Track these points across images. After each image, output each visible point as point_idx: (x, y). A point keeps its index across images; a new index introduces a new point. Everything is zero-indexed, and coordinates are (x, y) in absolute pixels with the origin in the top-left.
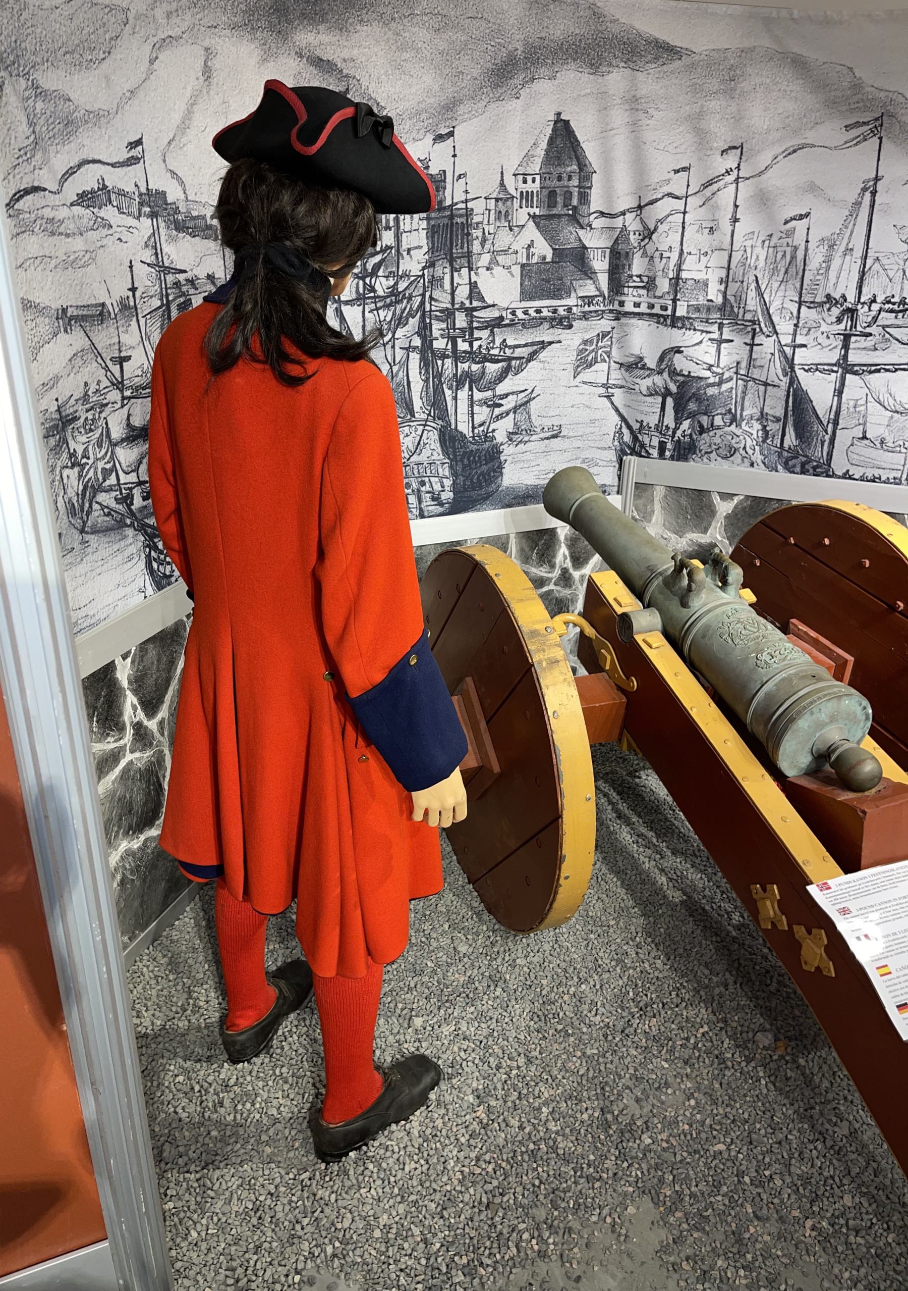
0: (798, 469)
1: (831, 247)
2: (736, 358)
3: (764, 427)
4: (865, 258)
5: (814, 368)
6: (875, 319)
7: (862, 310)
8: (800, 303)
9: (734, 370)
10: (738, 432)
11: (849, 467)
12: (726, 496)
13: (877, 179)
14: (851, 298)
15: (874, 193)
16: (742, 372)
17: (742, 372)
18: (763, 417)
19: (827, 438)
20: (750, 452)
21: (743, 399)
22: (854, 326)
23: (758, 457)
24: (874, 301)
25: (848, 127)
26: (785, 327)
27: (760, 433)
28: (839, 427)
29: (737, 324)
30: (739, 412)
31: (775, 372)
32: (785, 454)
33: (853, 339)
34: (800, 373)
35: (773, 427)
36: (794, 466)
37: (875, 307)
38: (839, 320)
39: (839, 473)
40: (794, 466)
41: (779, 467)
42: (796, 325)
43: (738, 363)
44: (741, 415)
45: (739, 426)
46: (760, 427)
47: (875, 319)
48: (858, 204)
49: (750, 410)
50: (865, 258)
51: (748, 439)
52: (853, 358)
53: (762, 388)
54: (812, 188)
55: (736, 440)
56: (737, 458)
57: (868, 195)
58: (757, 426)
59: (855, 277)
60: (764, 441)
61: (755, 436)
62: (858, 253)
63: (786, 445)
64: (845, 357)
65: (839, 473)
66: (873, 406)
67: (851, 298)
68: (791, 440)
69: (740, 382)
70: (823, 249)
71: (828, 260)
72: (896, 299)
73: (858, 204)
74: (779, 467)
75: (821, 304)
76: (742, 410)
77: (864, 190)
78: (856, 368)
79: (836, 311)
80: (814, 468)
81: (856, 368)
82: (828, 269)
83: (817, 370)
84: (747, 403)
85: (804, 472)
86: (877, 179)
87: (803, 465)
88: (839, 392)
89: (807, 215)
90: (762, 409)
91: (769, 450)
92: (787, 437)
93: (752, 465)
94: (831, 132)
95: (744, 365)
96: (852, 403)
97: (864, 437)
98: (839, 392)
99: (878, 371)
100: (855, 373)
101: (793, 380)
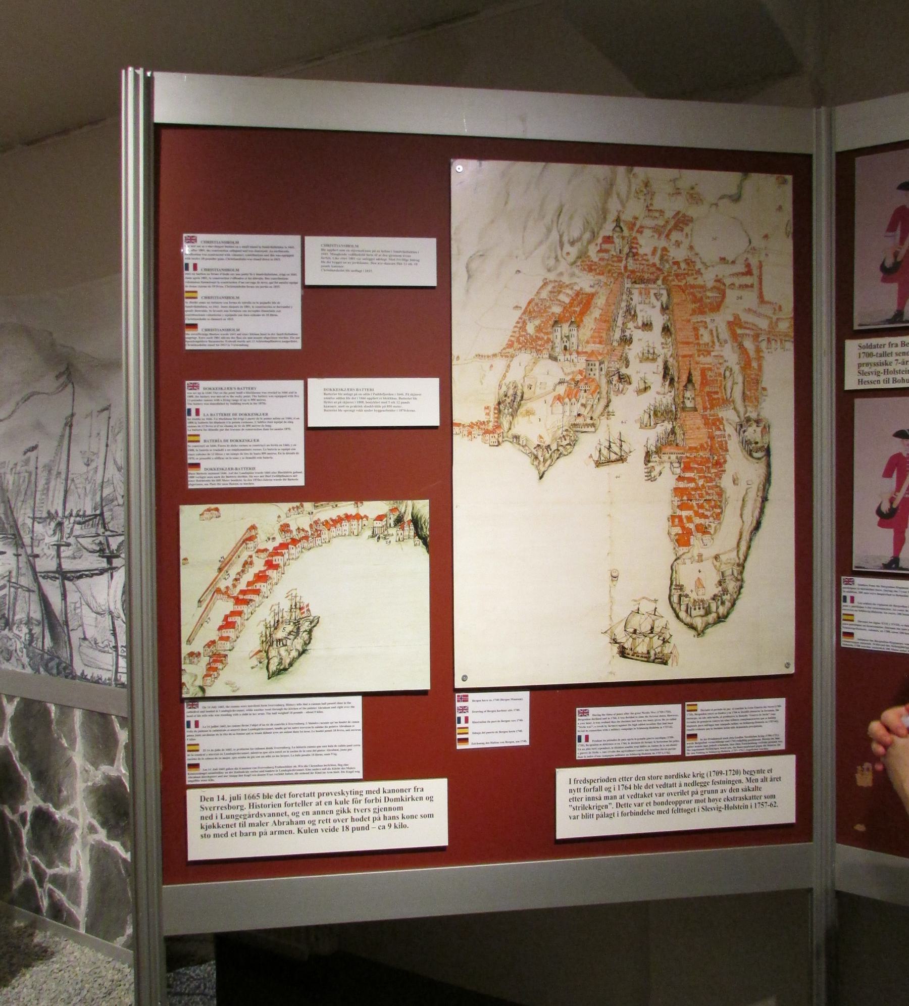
0: (55, 671)
1: (50, 471)
2: (8, 567)
3: (31, 630)
4: (67, 479)
5: (47, 575)
6: (72, 529)
7: (66, 523)
8: (34, 519)
9: (7, 579)
10: (10, 635)
11: (83, 667)
12: (10, 698)
13: (73, 415)
14: (60, 514)
15: (71, 426)
16: (13, 580)
17: (13, 580)
18: (29, 622)
19: (66, 638)
20: (20, 654)
21: (14, 604)
22: (62, 538)
23: (26, 660)
24: (71, 515)
25: (57, 377)
26: (27, 540)
27: (28, 636)
28: (71, 628)
29: (8, 538)
30: (11, 617)
31: (26, 581)
32: (46, 656)
33: (62, 548)
34: (41, 579)
35: (37, 630)
36: (52, 668)
37: (72, 519)
38: (54, 534)
39: (79, 674)
40: (52, 668)
41: (41, 669)
42: (32, 538)
43: (10, 572)
44: (13, 620)
45: (11, 629)
46: (27, 631)
47: (72, 529)
48: (62, 436)
49: (20, 616)
50: (67, 479)
51: (18, 643)
52: (67, 565)
53: (27, 593)
54: (39, 426)
55: (9, 643)
56: (13, 660)
57: (68, 428)
58: (25, 630)
59: (62, 494)
60: (30, 644)
61: (23, 639)
62: (63, 476)
63: (46, 648)
64: (60, 565)
65: (79, 674)
66: (85, 607)
67: (60, 514)
68: (48, 643)
69: (12, 590)
70: (45, 474)
71: (48, 483)
72: (81, 513)
73: (62, 436)
74: (41, 669)
75: (45, 519)
76: (14, 615)
77: (66, 425)
78: (69, 575)
79: (53, 525)
80: (65, 668)
81: (69, 575)
82: (48, 489)
83: (48, 577)
84: (17, 609)
85: (59, 673)
86: (73, 415)
87: (58, 665)
88: (64, 596)
89: (34, 448)
90: (29, 613)
91: (34, 652)
92: (46, 640)
93: (24, 667)
94: (49, 383)
95: (14, 574)
96: (73, 606)
97: (85, 639)
98: (64, 596)
99: (81, 577)
100: (69, 579)
101: (40, 588)
